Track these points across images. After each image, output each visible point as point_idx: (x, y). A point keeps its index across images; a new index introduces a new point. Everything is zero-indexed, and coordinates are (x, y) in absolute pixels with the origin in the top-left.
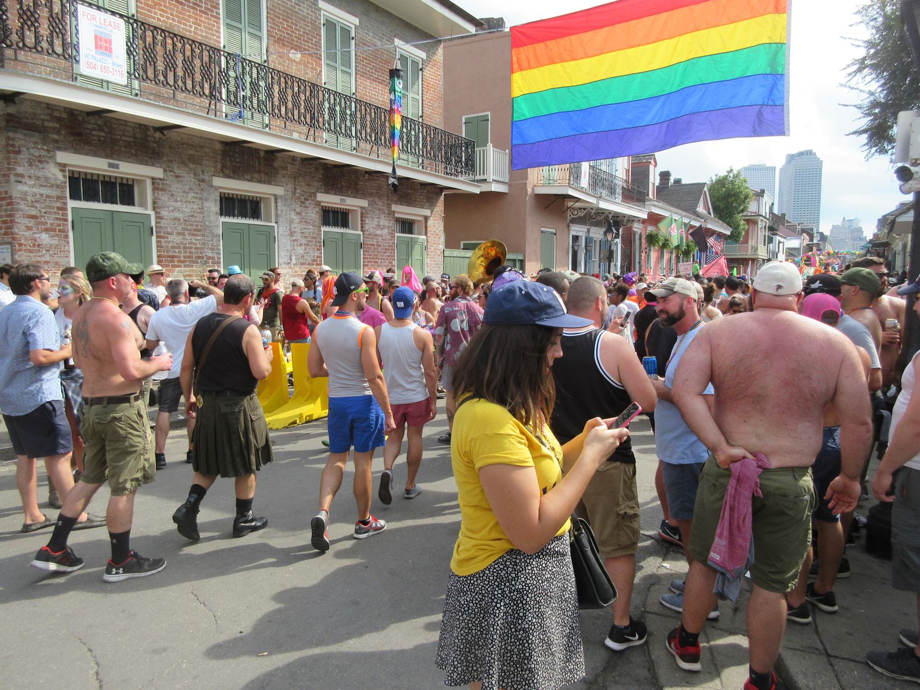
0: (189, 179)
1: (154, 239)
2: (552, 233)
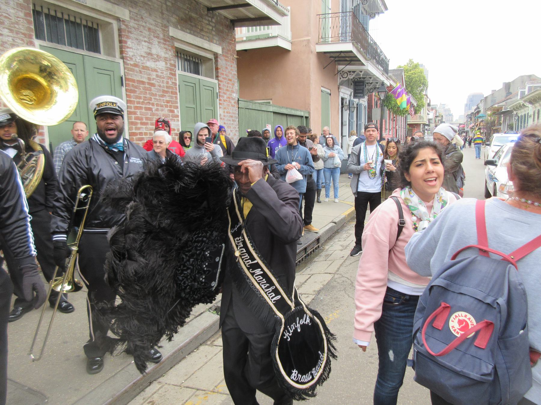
2: (328, 93)
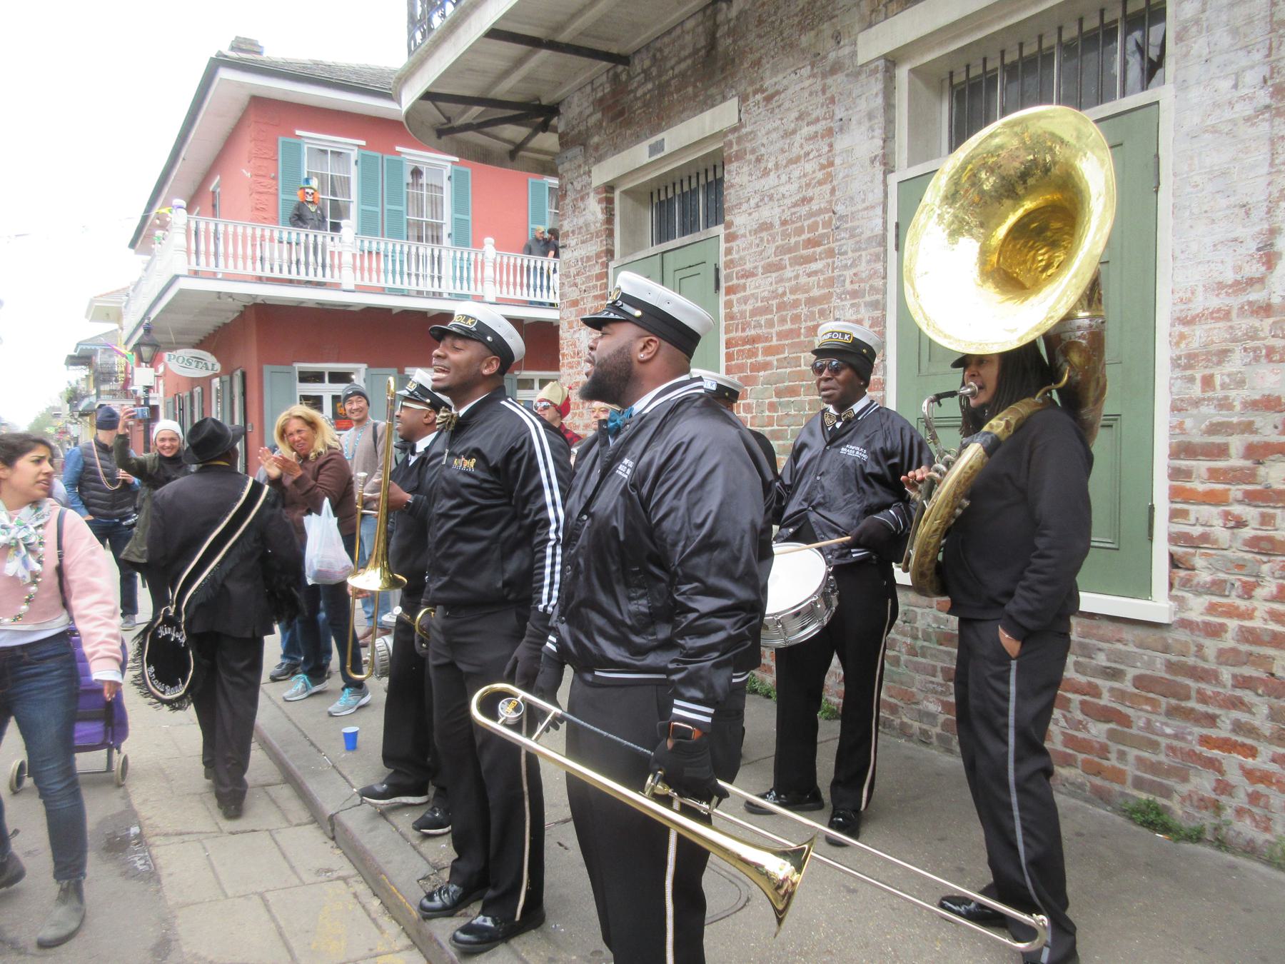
0: (794, 83)
1: (723, 298)
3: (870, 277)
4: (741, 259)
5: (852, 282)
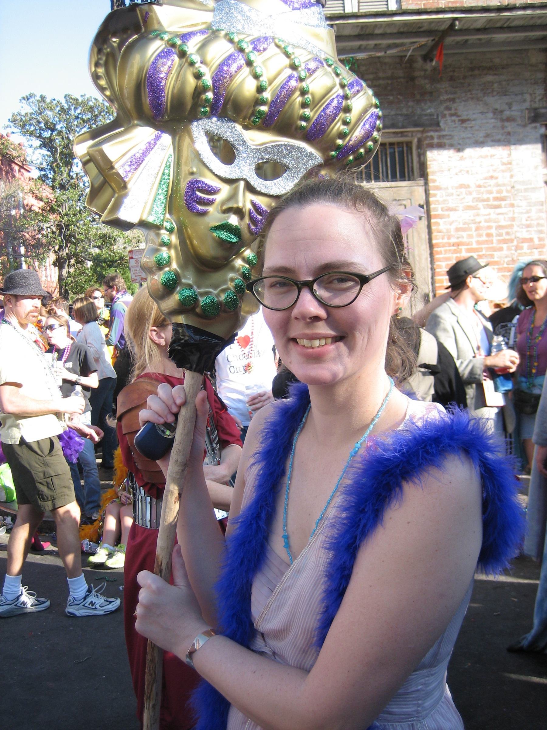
3: (537, 219)
4: (445, 200)
5: (527, 220)
